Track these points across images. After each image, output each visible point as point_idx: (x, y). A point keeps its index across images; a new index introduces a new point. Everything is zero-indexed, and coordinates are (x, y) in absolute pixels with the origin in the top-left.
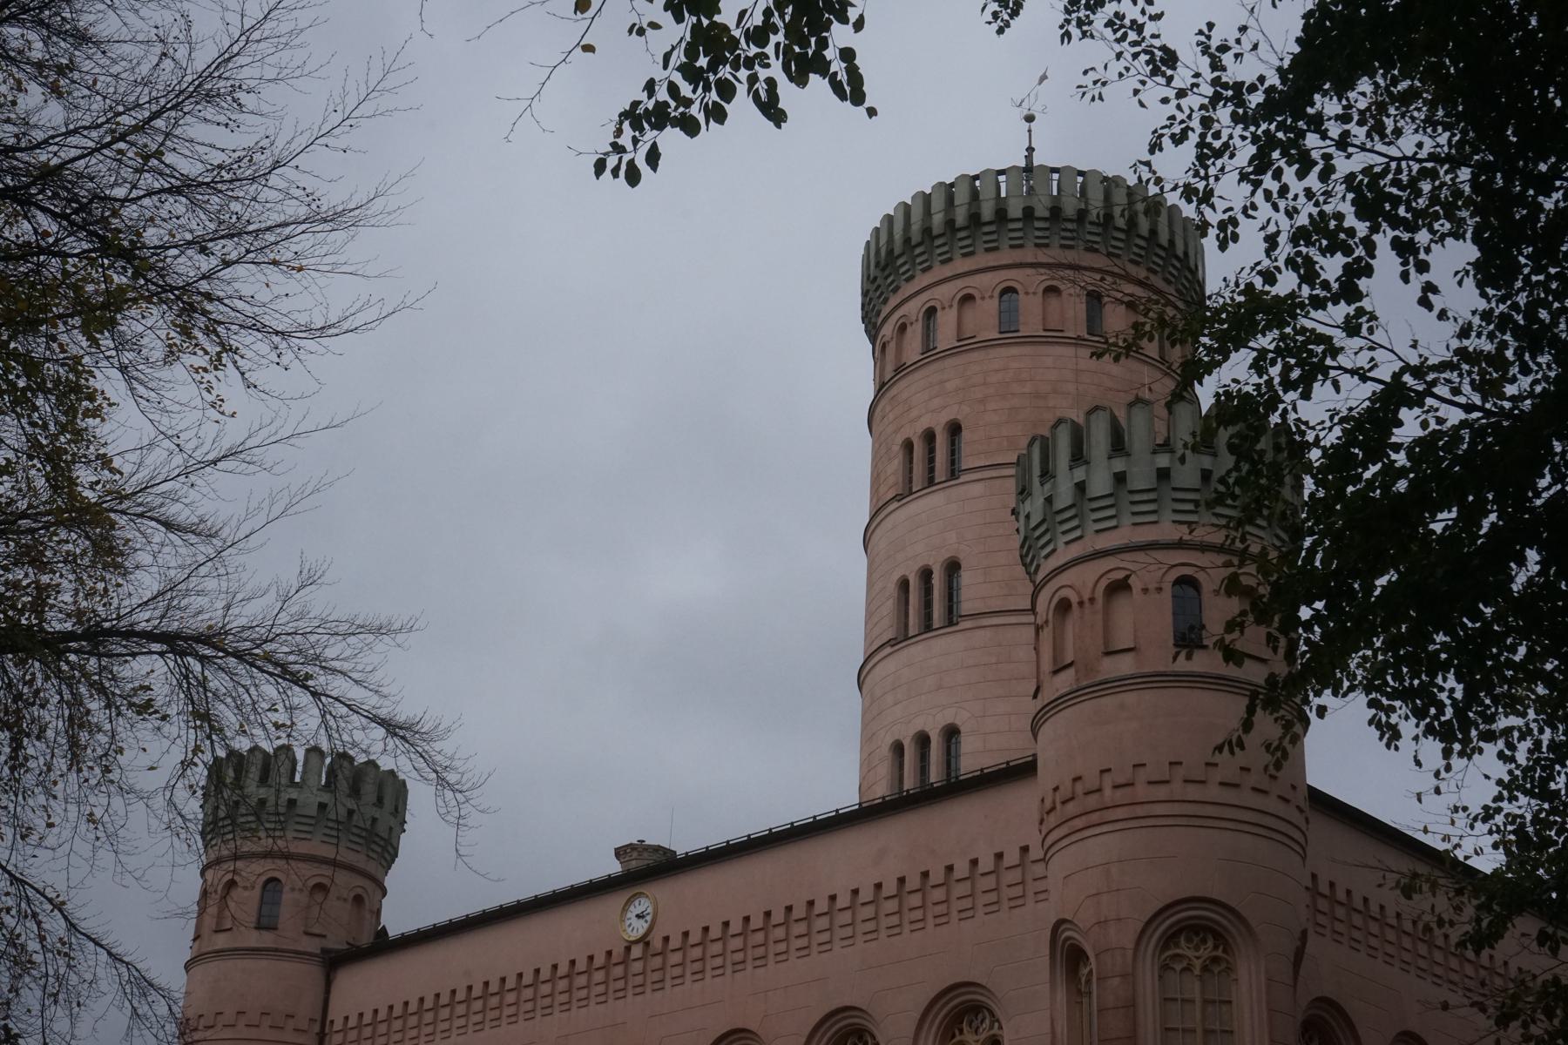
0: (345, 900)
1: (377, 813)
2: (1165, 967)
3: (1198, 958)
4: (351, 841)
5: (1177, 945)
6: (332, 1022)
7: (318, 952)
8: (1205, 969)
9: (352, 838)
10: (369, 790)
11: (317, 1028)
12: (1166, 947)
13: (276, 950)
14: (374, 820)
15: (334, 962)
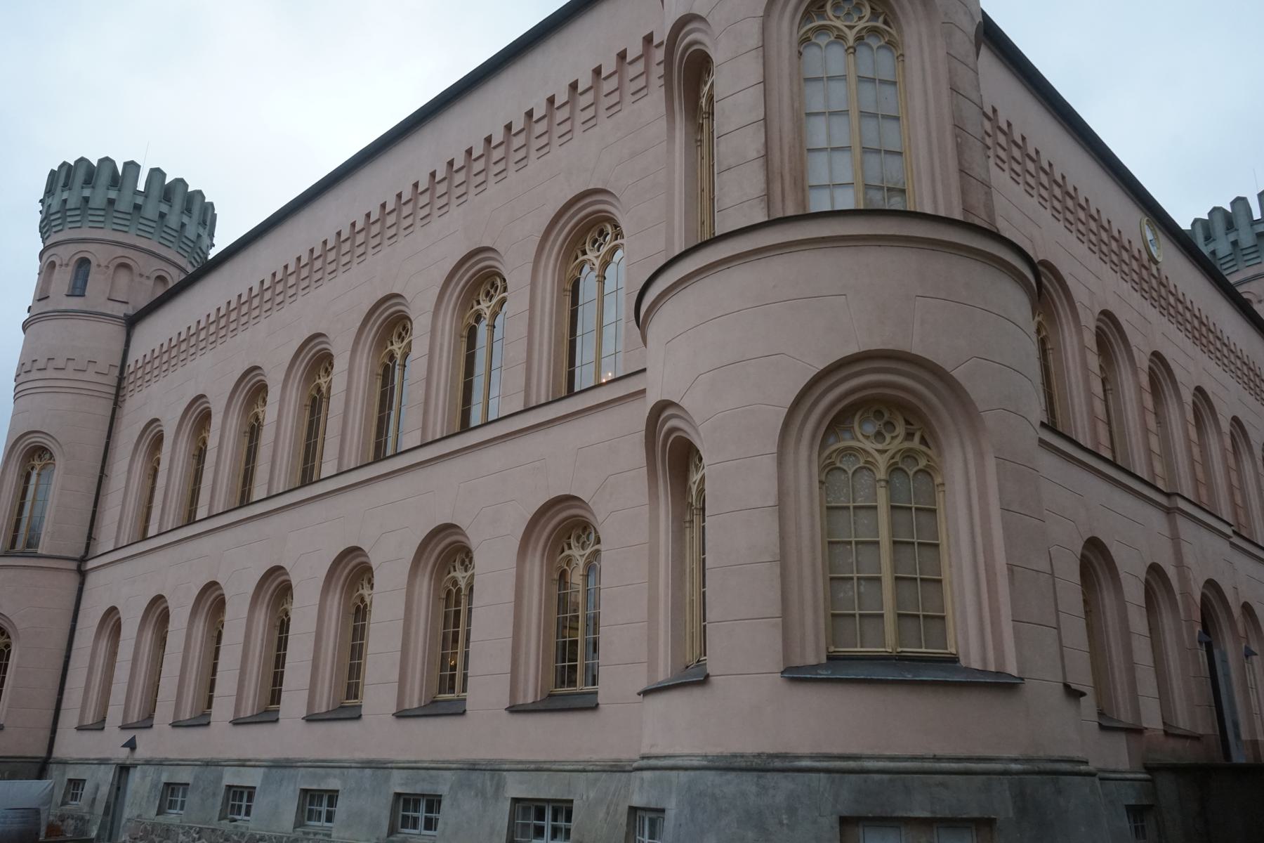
0: (148, 278)
1: (185, 219)
2: (805, 41)
3: (851, 28)
4: (162, 237)
5: (822, 15)
6: (129, 366)
7: (122, 315)
8: (859, 39)
9: (164, 235)
10: (178, 202)
11: (116, 372)
12: (807, 16)
13: (86, 312)
14: (183, 225)
15: (132, 322)
